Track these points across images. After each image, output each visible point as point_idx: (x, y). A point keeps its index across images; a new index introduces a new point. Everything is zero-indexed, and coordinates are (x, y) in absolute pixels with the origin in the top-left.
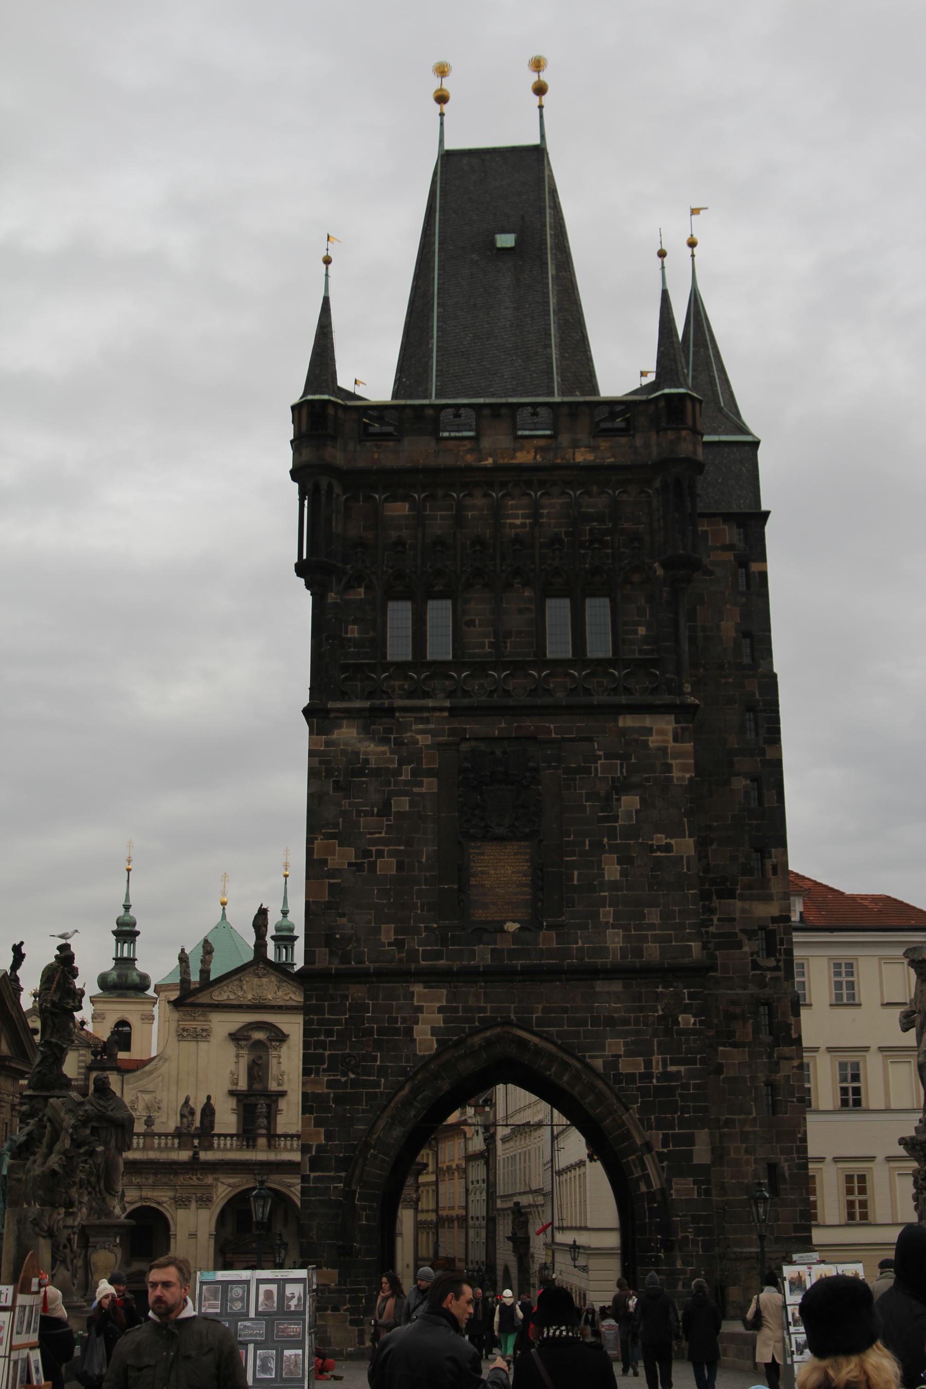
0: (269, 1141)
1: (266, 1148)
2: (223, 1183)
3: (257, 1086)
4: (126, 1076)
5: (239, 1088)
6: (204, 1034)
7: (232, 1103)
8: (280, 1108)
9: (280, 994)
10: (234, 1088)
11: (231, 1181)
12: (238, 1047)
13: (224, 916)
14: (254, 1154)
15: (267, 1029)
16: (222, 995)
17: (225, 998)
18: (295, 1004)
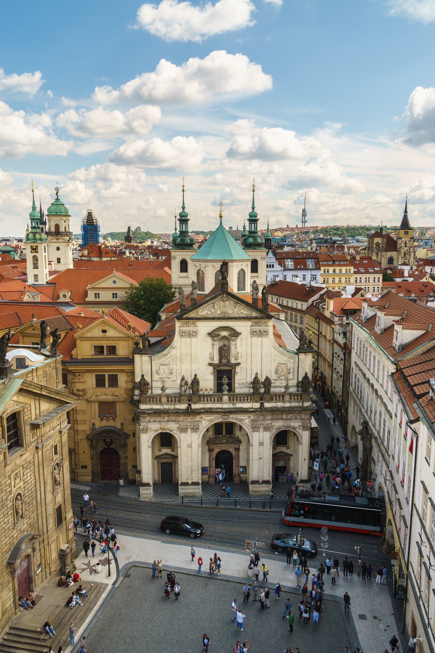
0: (230, 398)
1: (227, 401)
2: (205, 420)
3: (224, 361)
4: (154, 357)
5: (214, 362)
6: (194, 334)
7: (211, 369)
8: (237, 371)
9: (236, 310)
10: (212, 362)
11: (209, 418)
12: (214, 340)
13: (221, 222)
14: (221, 404)
15: (229, 330)
16: (203, 311)
17: (205, 313)
18: (244, 315)
